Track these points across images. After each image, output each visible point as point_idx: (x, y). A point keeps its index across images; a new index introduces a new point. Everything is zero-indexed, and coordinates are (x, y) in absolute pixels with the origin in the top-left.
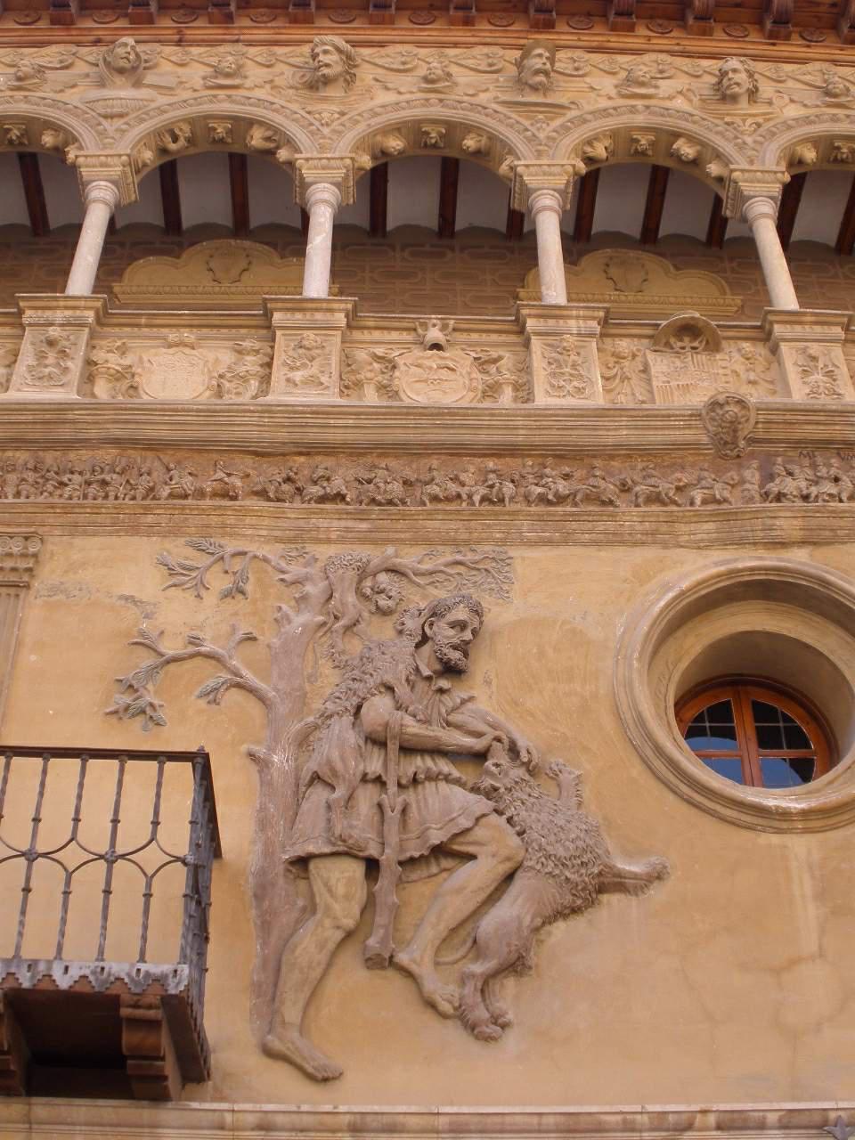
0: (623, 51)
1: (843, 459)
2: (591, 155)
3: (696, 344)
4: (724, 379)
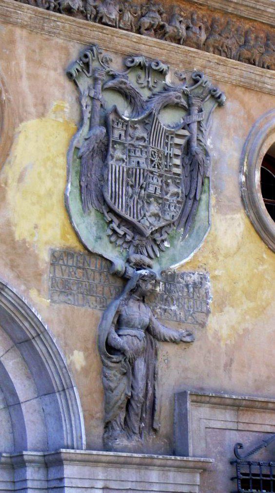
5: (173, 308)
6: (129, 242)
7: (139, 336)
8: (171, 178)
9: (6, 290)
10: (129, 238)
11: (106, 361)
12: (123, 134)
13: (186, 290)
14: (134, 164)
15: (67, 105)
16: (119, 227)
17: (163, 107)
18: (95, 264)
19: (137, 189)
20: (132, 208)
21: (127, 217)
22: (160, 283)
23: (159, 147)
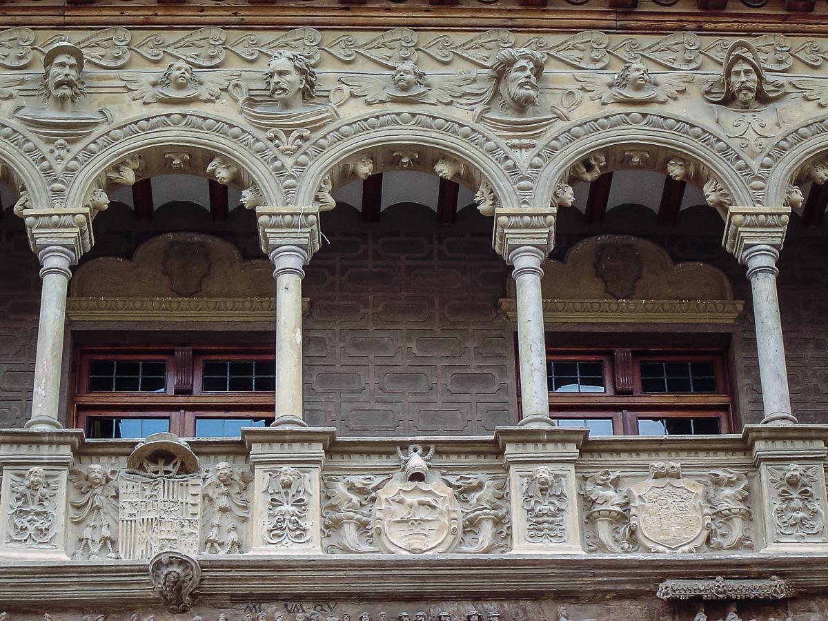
0: (170, 27)
1: (289, 612)
2: (118, 181)
3: (170, 468)
4: (192, 510)
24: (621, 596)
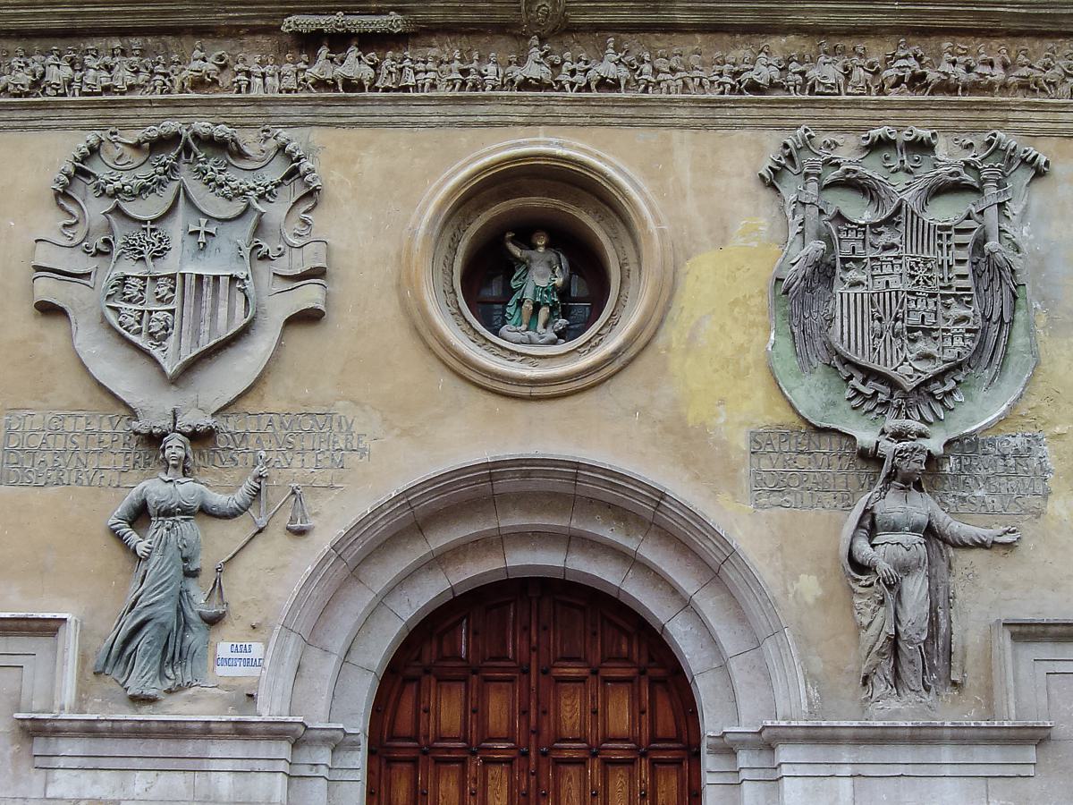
5: (978, 493)
6: (886, 404)
7: (904, 543)
8: (954, 296)
9: (667, 498)
10: (882, 397)
11: (854, 586)
12: (859, 245)
13: (1001, 462)
14: (882, 286)
15: (763, 221)
16: (864, 383)
17: (931, 194)
18: (828, 445)
19: (888, 322)
20: (882, 351)
21: (875, 366)
22: (949, 458)
23: (926, 250)
24: (254, 31)
